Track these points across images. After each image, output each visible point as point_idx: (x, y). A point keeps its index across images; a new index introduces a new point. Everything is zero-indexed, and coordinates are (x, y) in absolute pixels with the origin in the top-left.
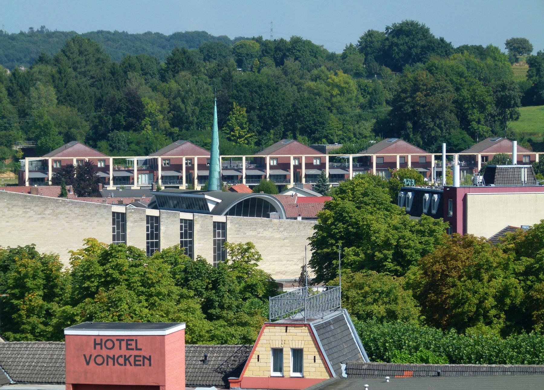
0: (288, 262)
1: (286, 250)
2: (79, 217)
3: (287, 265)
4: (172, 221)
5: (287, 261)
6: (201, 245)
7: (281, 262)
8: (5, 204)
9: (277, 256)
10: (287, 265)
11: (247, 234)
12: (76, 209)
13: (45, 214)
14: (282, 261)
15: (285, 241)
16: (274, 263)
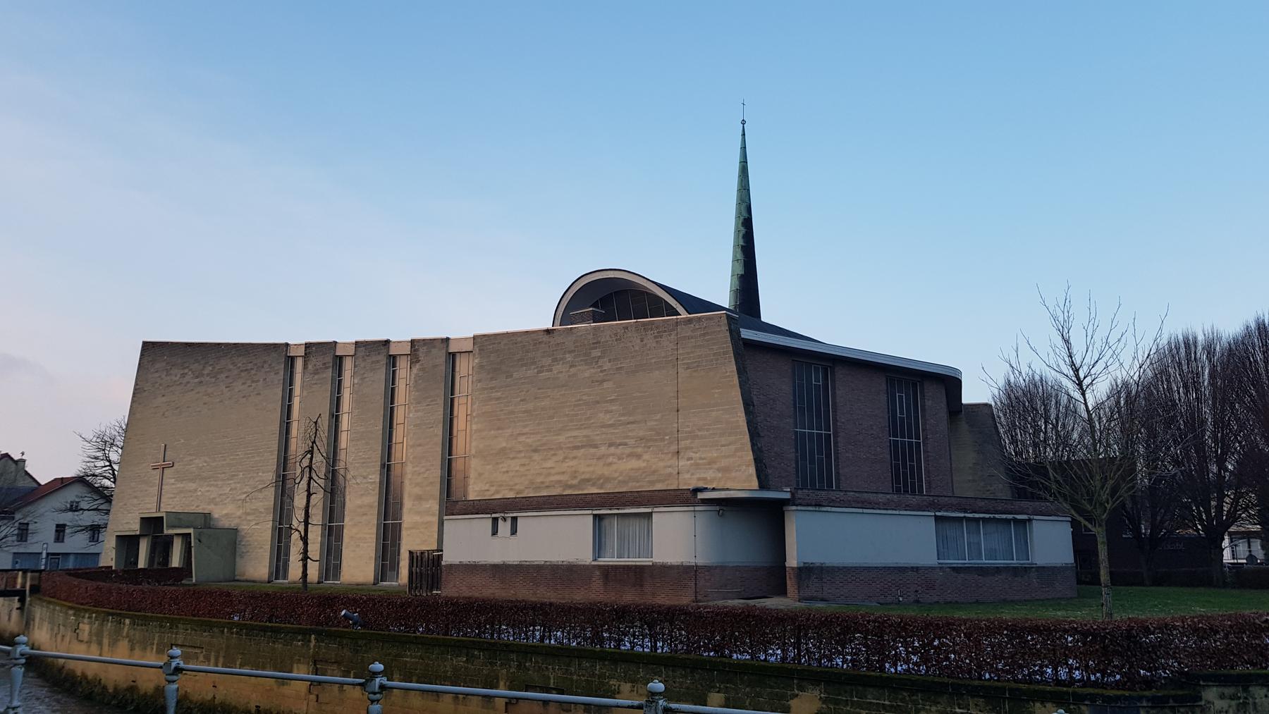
0: (612, 449)
1: (607, 412)
2: (243, 374)
3: (611, 459)
4: (373, 362)
5: (610, 445)
6: (419, 414)
7: (592, 450)
8: (164, 364)
9: (585, 432)
10: (611, 459)
11: (515, 375)
12: (240, 359)
13: (203, 375)
14: (596, 446)
15: (606, 385)
16: (575, 453)
